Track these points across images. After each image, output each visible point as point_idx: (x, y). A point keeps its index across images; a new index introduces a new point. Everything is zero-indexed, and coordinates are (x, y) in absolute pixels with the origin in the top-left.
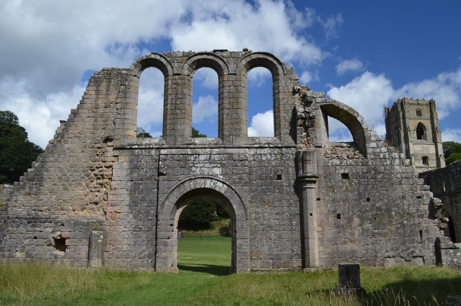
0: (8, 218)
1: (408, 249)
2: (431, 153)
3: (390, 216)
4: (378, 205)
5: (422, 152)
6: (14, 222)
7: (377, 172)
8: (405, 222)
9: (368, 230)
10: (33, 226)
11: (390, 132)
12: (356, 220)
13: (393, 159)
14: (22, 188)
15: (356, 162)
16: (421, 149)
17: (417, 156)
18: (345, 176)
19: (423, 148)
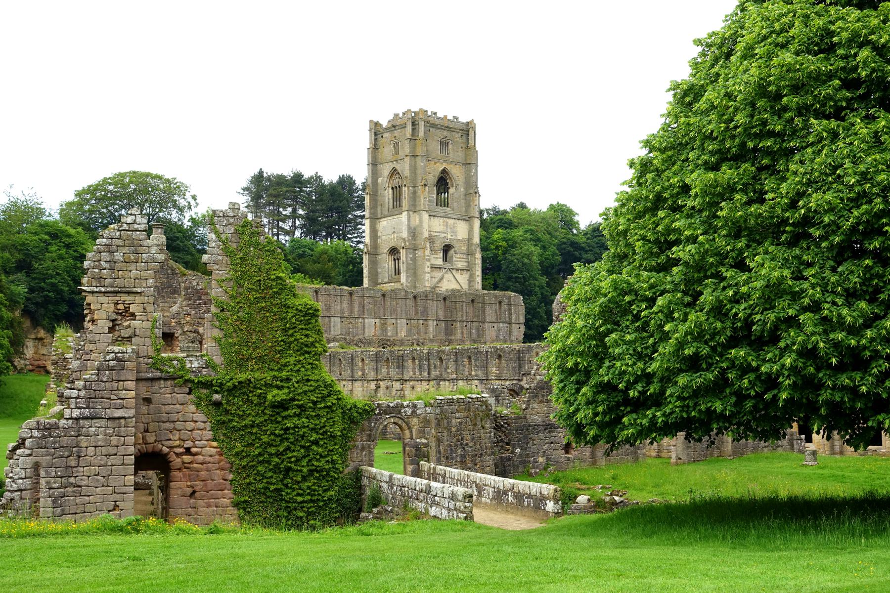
0: (530, 425)
2: (460, 238)
5: (443, 235)
6: (534, 429)
10: (550, 432)
14: (536, 396)
17: (434, 243)
19: (447, 226)
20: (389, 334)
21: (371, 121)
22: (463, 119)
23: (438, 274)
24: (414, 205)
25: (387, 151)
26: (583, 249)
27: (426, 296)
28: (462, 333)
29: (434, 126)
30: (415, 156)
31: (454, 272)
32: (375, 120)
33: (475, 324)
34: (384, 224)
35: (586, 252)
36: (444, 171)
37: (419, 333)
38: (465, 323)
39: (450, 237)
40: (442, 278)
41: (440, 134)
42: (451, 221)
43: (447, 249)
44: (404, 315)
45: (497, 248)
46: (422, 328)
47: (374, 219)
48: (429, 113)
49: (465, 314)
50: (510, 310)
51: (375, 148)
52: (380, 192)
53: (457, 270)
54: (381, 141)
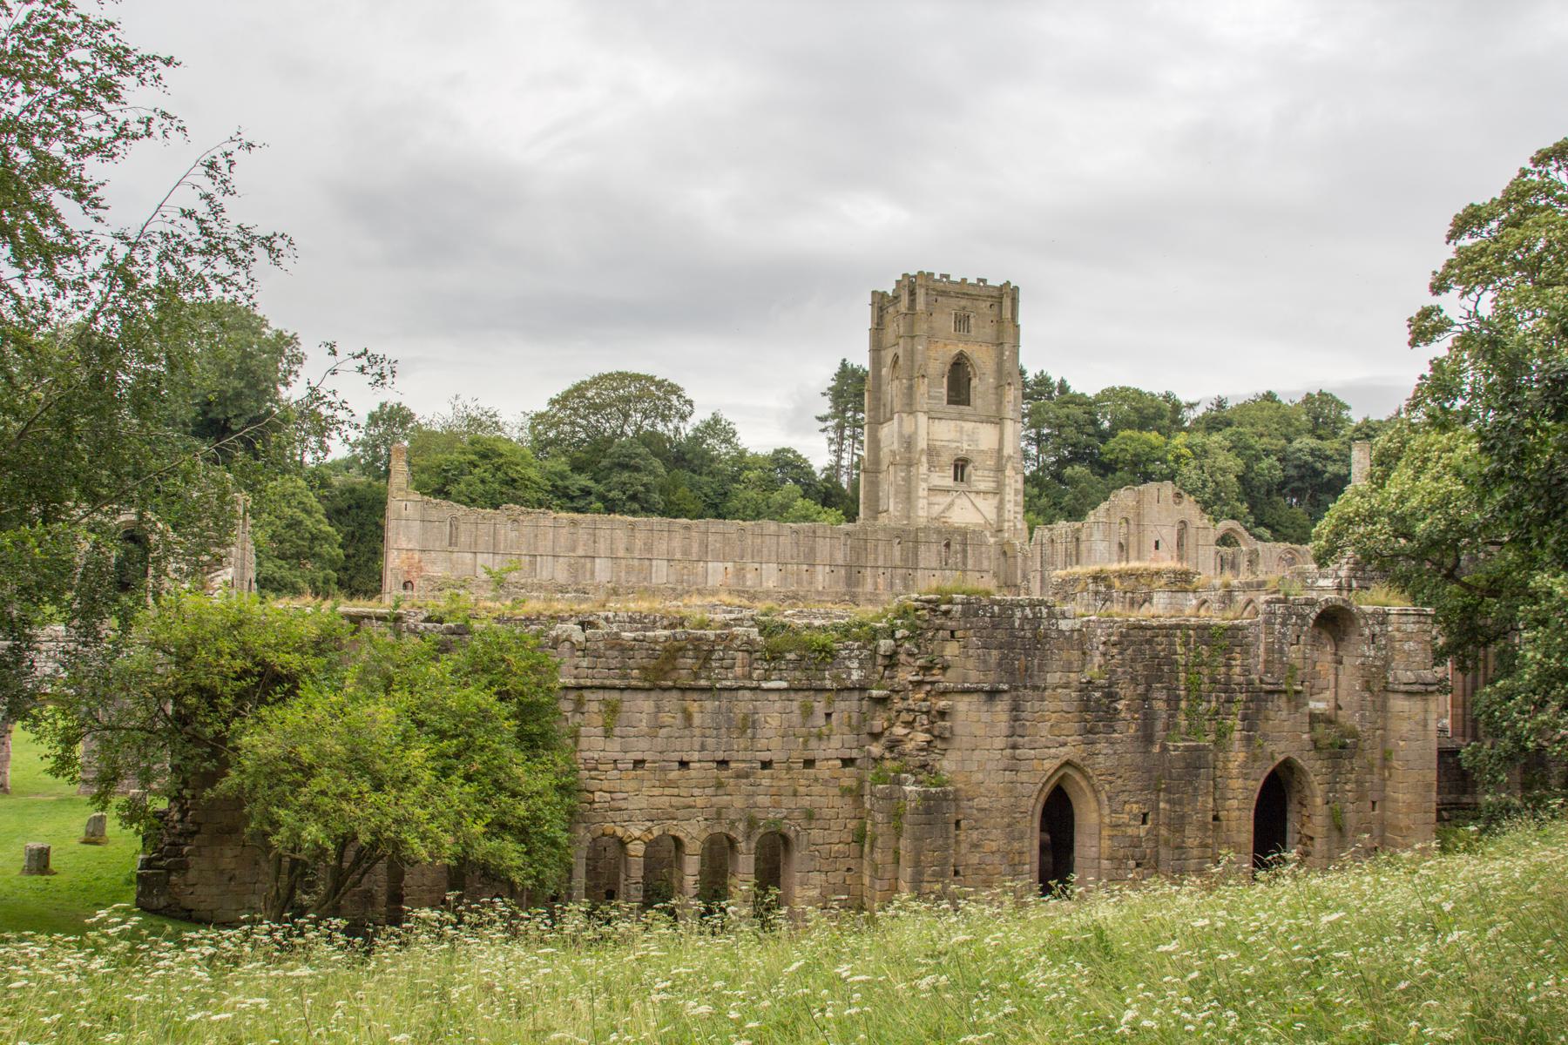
2: (983, 447)
16: (953, 435)
17: (938, 455)
19: (961, 431)
20: (749, 583)
22: (995, 281)
23: (944, 500)
24: (910, 404)
26: (1328, 458)
28: (876, 583)
29: (944, 293)
30: (913, 337)
31: (972, 496)
33: (899, 571)
35: (1335, 461)
37: (799, 582)
38: (881, 571)
39: (965, 446)
40: (951, 505)
41: (957, 304)
42: (968, 426)
43: (960, 467)
44: (774, 558)
45: (1178, 458)
46: (805, 576)
47: (877, 423)
49: (881, 557)
50: (964, 551)
53: (977, 493)
54: (888, 318)
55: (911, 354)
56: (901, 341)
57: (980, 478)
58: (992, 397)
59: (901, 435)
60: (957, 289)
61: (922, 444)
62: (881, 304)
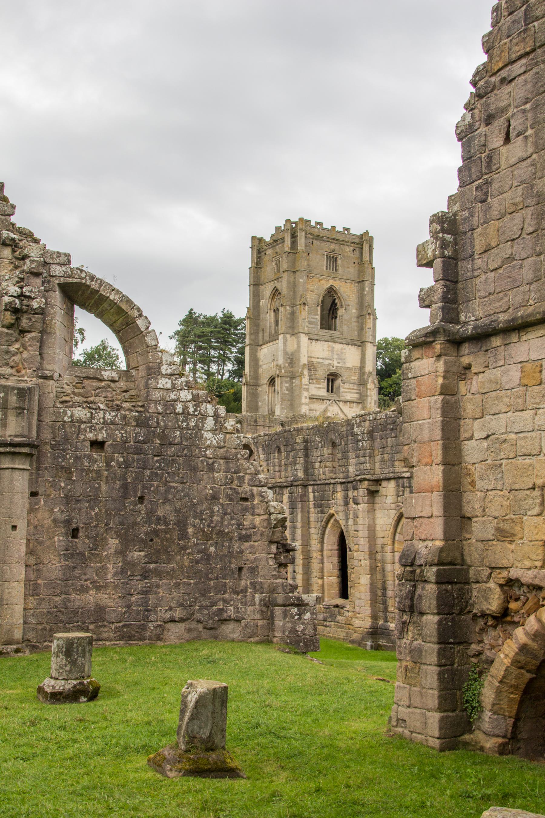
1: (214, 604)
2: (349, 365)
3: (183, 535)
4: (160, 513)
5: (327, 362)
7: (166, 442)
8: (212, 549)
9: (133, 565)
11: (259, 302)
12: (113, 543)
13: (204, 417)
15: (124, 417)
16: (326, 354)
17: (315, 370)
18: (97, 445)
19: (332, 351)
21: (253, 238)
22: (357, 230)
24: (293, 327)
25: (269, 270)
27: (256, 421)
29: (318, 237)
30: (294, 272)
31: (341, 404)
32: (259, 236)
34: (264, 352)
36: (331, 292)
42: (338, 347)
43: (332, 379)
47: (256, 345)
48: (313, 224)
51: (257, 267)
52: (262, 316)
53: (345, 402)
54: (265, 259)
55: (293, 286)
56: (285, 275)
57: (348, 391)
58: (354, 325)
59: (285, 353)
60: (328, 234)
61: (304, 360)
62: (259, 247)
